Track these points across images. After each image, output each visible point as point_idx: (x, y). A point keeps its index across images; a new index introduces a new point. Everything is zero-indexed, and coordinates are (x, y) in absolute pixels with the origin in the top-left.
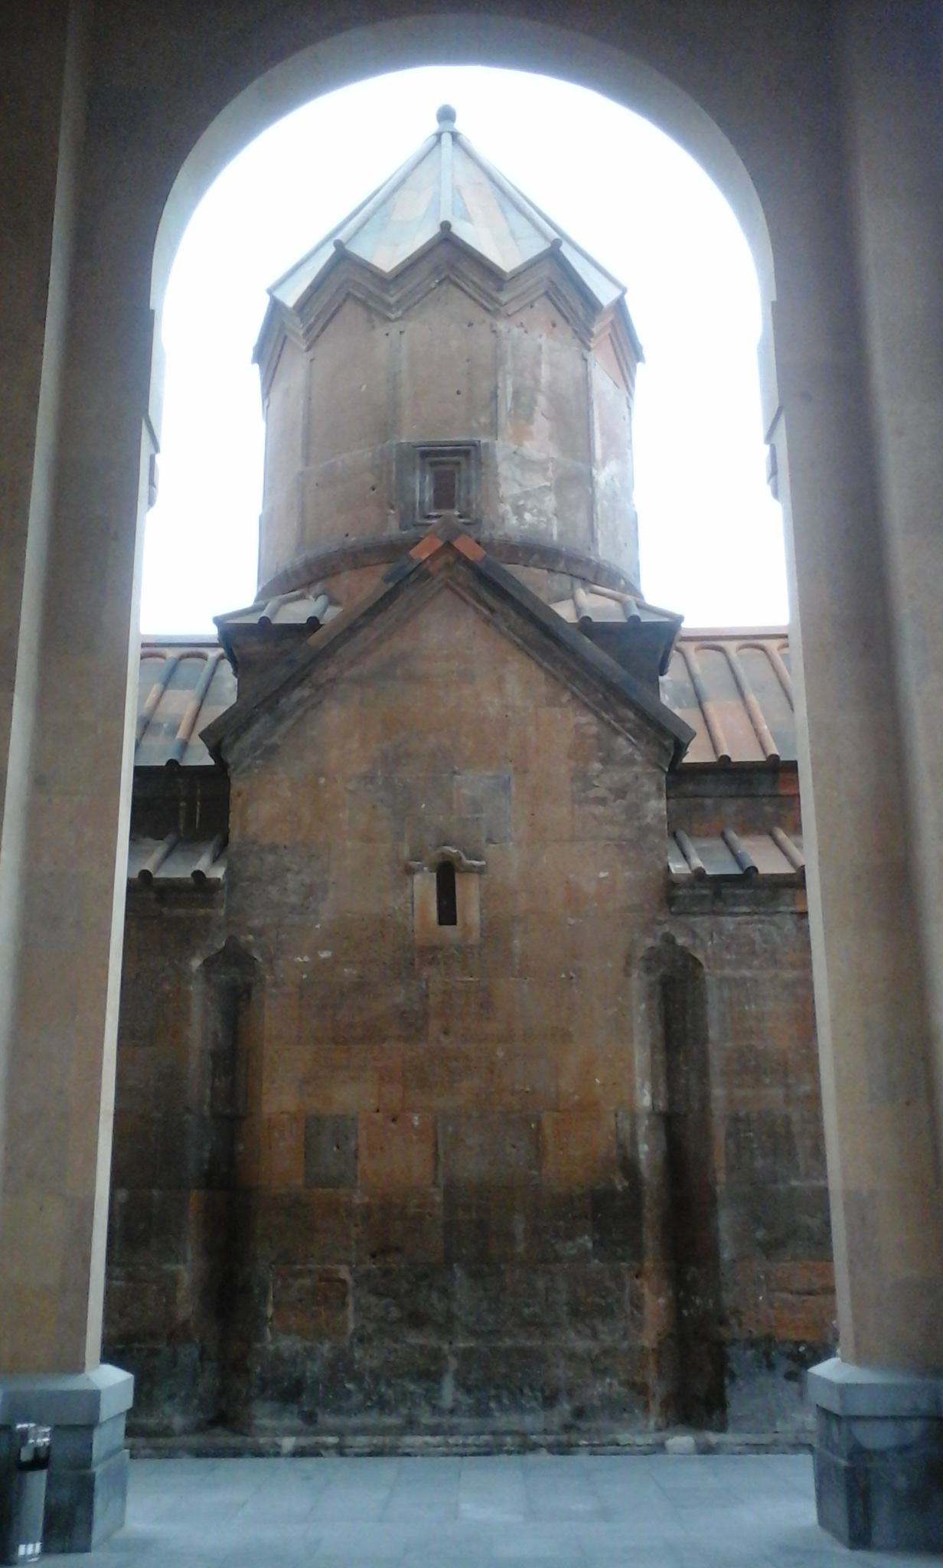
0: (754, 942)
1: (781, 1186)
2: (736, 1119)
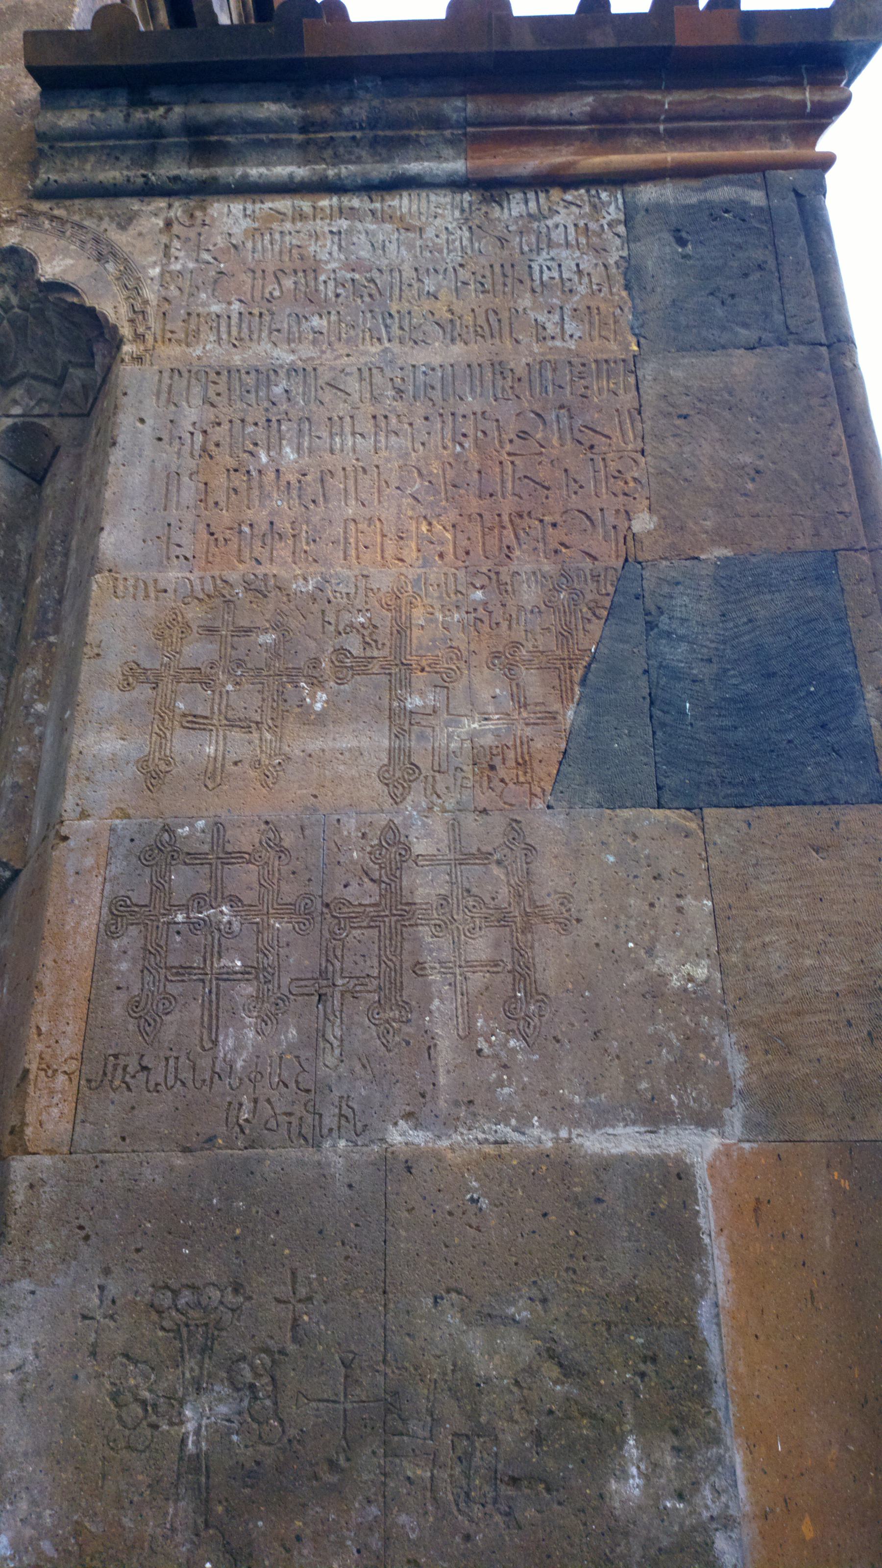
0: (311, 269)
1: (337, 1150)
2: (160, 851)
